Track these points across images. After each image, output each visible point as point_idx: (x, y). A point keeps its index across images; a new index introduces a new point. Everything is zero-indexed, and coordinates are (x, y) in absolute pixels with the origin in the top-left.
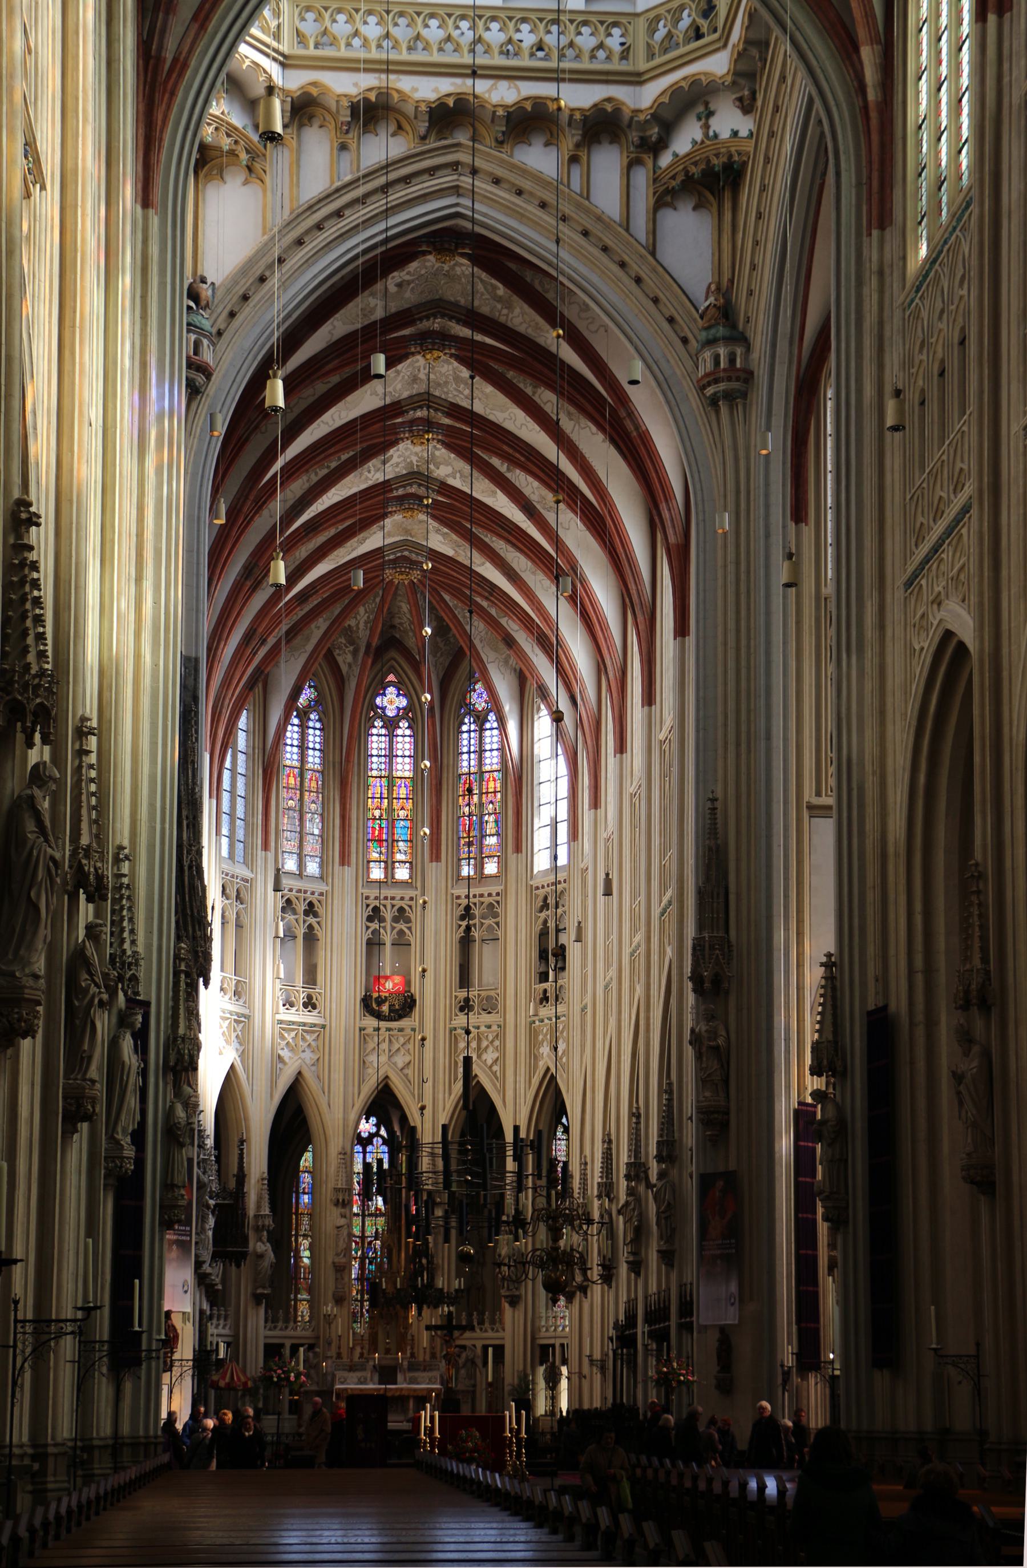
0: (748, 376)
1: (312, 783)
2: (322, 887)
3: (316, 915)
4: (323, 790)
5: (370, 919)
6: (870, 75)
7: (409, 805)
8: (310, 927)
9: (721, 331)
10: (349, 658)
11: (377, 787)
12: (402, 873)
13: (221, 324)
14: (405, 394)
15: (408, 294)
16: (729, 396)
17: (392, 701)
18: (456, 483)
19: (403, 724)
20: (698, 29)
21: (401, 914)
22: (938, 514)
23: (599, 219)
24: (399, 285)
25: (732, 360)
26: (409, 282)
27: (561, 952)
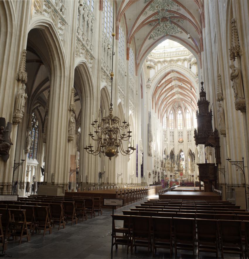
8: (173, 134)
11: (179, 121)
12: (182, 129)
13: (152, 82)
17: (180, 112)
19: (181, 114)
23: (185, 68)
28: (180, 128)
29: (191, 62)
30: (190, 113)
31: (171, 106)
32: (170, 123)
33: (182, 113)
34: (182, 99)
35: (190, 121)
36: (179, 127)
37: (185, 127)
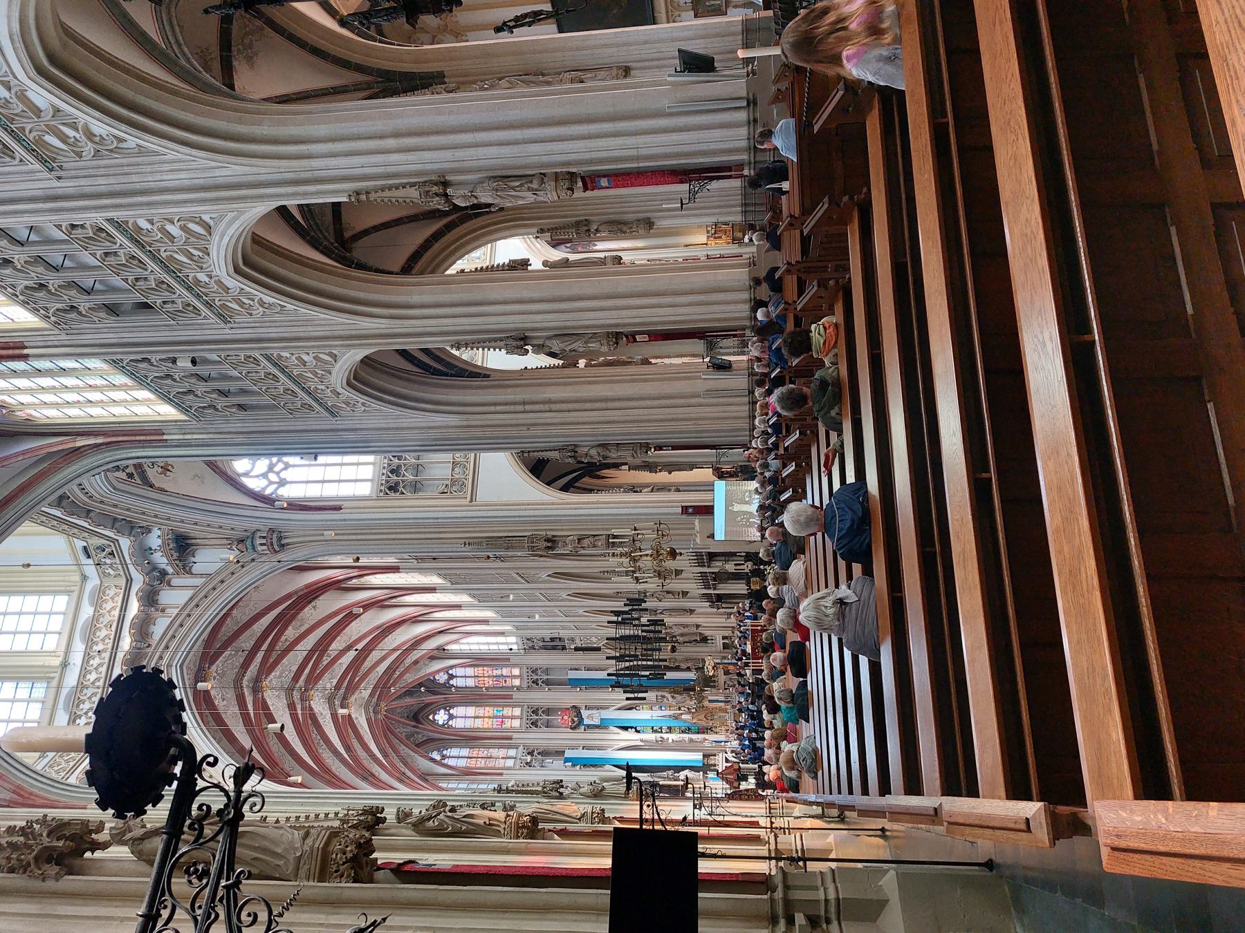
0: (272, 530)
1: (475, 753)
2: (521, 748)
3: (533, 751)
4: (479, 747)
5: (536, 726)
6: (91, 441)
7: (487, 708)
8: (539, 754)
9: (249, 542)
10: (420, 736)
11: (478, 723)
12: (517, 711)
14: (285, 701)
15: (229, 696)
16: (280, 539)
17: (441, 717)
18: (335, 681)
19: (451, 711)
20: (110, 554)
21: (535, 712)
22: (294, 393)
23: (191, 599)
24: (223, 700)
25: (264, 537)
26: (223, 695)
27: (552, 639)
28: (513, 718)
29: (170, 570)
30: (452, 667)
31: (404, 750)
32: (483, 765)
33: (447, 706)
34: (382, 686)
35: (489, 671)
36: (508, 723)
37: (510, 697)
